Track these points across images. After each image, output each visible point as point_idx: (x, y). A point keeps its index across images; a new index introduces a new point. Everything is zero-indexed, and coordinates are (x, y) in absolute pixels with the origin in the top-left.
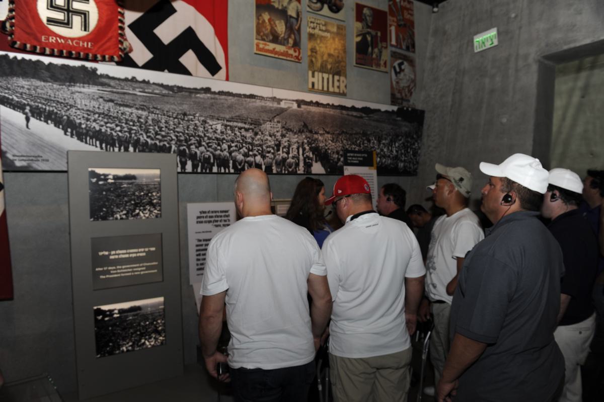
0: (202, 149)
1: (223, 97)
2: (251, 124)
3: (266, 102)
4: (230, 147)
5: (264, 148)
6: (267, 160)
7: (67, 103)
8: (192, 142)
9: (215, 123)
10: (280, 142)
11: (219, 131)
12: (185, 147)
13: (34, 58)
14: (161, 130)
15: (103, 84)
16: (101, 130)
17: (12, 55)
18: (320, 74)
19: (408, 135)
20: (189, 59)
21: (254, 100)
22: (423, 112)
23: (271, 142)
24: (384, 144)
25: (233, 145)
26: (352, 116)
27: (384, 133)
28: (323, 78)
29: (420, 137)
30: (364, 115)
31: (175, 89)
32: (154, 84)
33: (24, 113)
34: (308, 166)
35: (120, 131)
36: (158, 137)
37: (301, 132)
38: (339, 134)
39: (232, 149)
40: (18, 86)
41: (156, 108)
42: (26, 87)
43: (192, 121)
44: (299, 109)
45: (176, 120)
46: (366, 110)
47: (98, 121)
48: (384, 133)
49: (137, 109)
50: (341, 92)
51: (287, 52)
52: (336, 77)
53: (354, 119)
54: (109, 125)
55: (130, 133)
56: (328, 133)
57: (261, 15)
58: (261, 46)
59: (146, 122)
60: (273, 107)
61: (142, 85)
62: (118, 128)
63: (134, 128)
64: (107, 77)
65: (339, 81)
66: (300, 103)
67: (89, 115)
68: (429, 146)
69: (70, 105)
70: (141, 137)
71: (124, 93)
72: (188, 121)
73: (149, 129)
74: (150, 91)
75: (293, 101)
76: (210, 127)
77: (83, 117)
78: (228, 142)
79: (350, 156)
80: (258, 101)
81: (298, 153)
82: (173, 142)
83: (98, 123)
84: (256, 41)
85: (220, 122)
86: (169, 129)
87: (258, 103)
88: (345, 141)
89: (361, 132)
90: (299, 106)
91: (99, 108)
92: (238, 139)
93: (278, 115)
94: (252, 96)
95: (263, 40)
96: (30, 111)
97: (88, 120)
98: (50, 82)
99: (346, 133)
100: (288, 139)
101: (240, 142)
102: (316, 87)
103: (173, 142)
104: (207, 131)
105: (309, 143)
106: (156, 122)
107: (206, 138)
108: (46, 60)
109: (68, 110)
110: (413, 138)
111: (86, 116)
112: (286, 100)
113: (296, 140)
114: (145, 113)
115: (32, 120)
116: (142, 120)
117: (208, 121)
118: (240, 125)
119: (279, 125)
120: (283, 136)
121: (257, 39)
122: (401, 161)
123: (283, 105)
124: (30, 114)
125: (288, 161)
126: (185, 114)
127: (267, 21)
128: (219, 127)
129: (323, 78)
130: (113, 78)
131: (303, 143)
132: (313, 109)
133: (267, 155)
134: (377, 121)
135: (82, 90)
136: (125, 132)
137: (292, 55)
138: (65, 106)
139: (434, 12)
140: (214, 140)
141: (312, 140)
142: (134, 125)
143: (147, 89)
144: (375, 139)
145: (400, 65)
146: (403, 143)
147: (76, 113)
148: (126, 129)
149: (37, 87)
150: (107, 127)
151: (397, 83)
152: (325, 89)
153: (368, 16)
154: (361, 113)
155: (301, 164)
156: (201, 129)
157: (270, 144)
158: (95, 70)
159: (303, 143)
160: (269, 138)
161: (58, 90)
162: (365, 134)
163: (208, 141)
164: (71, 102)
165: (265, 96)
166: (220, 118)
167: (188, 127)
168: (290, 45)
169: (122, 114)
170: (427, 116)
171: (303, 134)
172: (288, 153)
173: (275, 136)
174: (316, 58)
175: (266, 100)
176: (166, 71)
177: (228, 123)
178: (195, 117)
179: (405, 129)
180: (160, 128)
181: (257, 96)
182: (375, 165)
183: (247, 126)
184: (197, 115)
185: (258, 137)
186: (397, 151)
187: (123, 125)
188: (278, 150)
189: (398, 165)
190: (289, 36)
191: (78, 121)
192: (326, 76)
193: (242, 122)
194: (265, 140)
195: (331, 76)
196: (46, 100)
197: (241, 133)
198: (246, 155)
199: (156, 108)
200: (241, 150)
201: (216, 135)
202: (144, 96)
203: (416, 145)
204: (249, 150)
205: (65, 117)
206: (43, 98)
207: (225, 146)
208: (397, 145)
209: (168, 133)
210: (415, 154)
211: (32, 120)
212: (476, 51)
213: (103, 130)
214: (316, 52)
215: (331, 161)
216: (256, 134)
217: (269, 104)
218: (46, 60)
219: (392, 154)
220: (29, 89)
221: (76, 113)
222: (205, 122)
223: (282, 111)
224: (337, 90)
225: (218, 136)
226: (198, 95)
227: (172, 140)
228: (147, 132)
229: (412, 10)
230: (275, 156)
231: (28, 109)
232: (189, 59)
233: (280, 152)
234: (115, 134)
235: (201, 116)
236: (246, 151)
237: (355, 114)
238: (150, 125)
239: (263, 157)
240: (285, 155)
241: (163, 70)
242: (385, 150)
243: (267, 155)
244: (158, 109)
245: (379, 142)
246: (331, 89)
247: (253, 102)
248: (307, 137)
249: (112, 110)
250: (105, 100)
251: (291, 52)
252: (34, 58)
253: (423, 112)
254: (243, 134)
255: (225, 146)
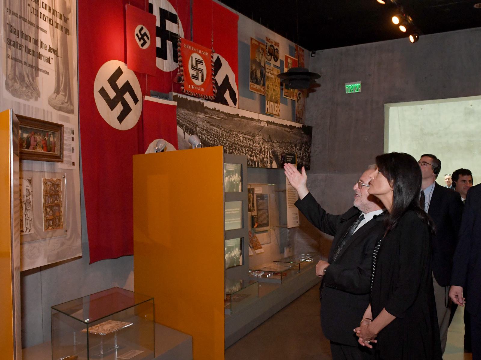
0: (237, 151)
1: (243, 120)
2: (252, 136)
3: (257, 122)
4: (245, 150)
5: (256, 151)
6: (258, 159)
7: (196, 124)
8: (234, 147)
9: (241, 136)
10: (261, 147)
11: (242, 141)
12: (231, 151)
13: (185, 97)
14: (224, 140)
15: (206, 113)
16: (206, 139)
17: (179, 95)
18: (270, 102)
19: (306, 143)
20: (227, 95)
21: (252, 121)
22: (312, 128)
23: (259, 149)
24: (297, 149)
25: (246, 149)
26: (286, 131)
27: (297, 142)
28: (271, 105)
29: (310, 144)
30: (290, 130)
31: (228, 115)
32: (221, 112)
33: (183, 130)
34: (271, 163)
35: (212, 140)
36: (223, 144)
37: (268, 141)
38: (282, 143)
39: (246, 152)
40: (181, 114)
41: (222, 127)
42: (183, 114)
43: (233, 135)
44: (267, 127)
45: (228, 134)
46: (291, 126)
47: (205, 135)
48: (297, 142)
49: (216, 127)
50: (278, 114)
51: (261, 89)
52: (276, 104)
53: (287, 133)
54: (208, 137)
55: (215, 142)
56: (278, 142)
57: (252, 67)
58: (252, 86)
59: (219, 135)
60: (259, 126)
61: (218, 113)
62: (211, 139)
63: (216, 139)
64: (206, 107)
65: (277, 107)
66: (268, 123)
67: (202, 131)
68: (315, 151)
69: (197, 125)
70: (218, 144)
71: (213, 118)
72: (232, 134)
73: (220, 139)
74: (220, 116)
75: (266, 121)
76: (239, 138)
77: (200, 132)
78: (245, 147)
79: (287, 158)
80: (254, 122)
81: (268, 155)
82: (228, 147)
83: (205, 136)
84: (250, 83)
85: (242, 135)
86: (226, 139)
87: (254, 123)
88: (283, 147)
89: (289, 142)
90: (267, 125)
91: (205, 127)
92: (248, 146)
93: (261, 130)
94: (252, 119)
95: (253, 82)
96: (185, 128)
97: (202, 134)
98: (190, 111)
99: (284, 142)
100: (264, 146)
101: (248, 148)
102: (268, 112)
103: (228, 147)
104: (238, 140)
105: (271, 149)
106: (222, 135)
107: (238, 145)
108: (189, 98)
109: (196, 127)
110: (308, 146)
111: (201, 131)
112: (263, 121)
113: (267, 146)
114: (219, 130)
115: (185, 133)
116: (218, 134)
117: (238, 135)
118: (248, 137)
119: (261, 137)
120: (263, 144)
121: (251, 82)
122: (305, 161)
123: (262, 125)
124: (185, 130)
125: (264, 159)
126: (231, 131)
127: (254, 70)
128: (242, 138)
129: (271, 105)
130: (209, 109)
131: (269, 148)
132: (273, 127)
133: (258, 156)
134: (295, 134)
135: (201, 116)
136: (213, 141)
137: (262, 91)
138: (195, 126)
139: (312, 56)
140: (240, 146)
141: (273, 147)
142: (215, 137)
143: (220, 115)
144: (294, 145)
145: (299, 94)
146: (304, 149)
147: (198, 129)
148: (213, 139)
149: (186, 114)
150: (208, 138)
151: (298, 107)
152: (272, 113)
153: (290, 63)
154: (289, 129)
155: (269, 162)
156: (236, 139)
157: (258, 149)
158: (203, 104)
159: (269, 148)
160: (258, 145)
161: (193, 116)
162: (291, 143)
163: (238, 147)
164: (197, 124)
165: (256, 119)
166: (242, 133)
167: (232, 139)
168: (262, 85)
169: (212, 130)
170: (313, 129)
171: (269, 142)
172: (264, 155)
173: (260, 143)
174: (269, 92)
175: (257, 121)
176: (220, 103)
177: (245, 136)
178: (234, 132)
179: (305, 140)
180: (224, 139)
181: (254, 119)
182: (296, 163)
183: (250, 138)
184: (235, 131)
185: (254, 144)
186: (302, 154)
187: (212, 137)
188: (261, 153)
189: (303, 163)
190: (261, 80)
191: (199, 134)
192: (272, 103)
193: (249, 135)
194: (257, 147)
195: (274, 103)
196: (190, 122)
197: (248, 142)
198: (251, 156)
199: (222, 127)
200: (249, 153)
201: (241, 143)
202: (219, 119)
203: (309, 150)
204: (252, 153)
205: (195, 132)
206: (188, 121)
207: (244, 150)
208: (302, 150)
209: (226, 142)
210: (309, 156)
211: (185, 133)
212: (347, 93)
213: (207, 140)
214: (269, 89)
215: (279, 160)
216: (254, 143)
217: (257, 124)
218: (189, 98)
219: (300, 156)
220: (184, 115)
221: (198, 129)
222: (237, 135)
223: (262, 127)
224: (276, 114)
225: (242, 144)
226: (235, 119)
227: (228, 146)
228: (220, 141)
229: (303, 56)
230: (260, 157)
231: (184, 128)
232: (227, 95)
233: (262, 154)
234: (210, 142)
235: (236, 132)
236: (251, 153)
237: (287, 129)
238: (221, 137)
239: (256, 157)
240: (263, 156)
241: (218, 103)
242: (298, 153)
243: (258, 156)
244: (223, 127)
245: (296, 148)
246: (274, 113)
247: (253, 123)
248: (271, 145)
249: (209, 128)
250: (207, 122)
251: (262, 89)
252: (185, 97)
253: (312, 128)
254: (249, 142)
255: (244, 150)
